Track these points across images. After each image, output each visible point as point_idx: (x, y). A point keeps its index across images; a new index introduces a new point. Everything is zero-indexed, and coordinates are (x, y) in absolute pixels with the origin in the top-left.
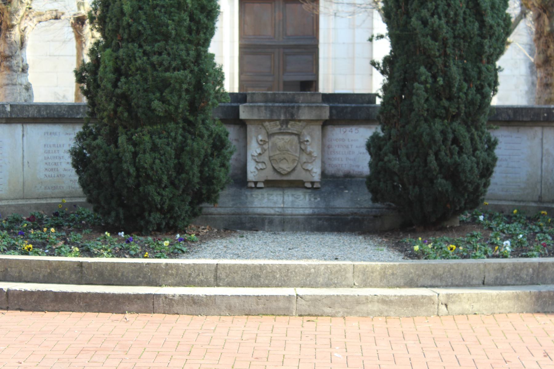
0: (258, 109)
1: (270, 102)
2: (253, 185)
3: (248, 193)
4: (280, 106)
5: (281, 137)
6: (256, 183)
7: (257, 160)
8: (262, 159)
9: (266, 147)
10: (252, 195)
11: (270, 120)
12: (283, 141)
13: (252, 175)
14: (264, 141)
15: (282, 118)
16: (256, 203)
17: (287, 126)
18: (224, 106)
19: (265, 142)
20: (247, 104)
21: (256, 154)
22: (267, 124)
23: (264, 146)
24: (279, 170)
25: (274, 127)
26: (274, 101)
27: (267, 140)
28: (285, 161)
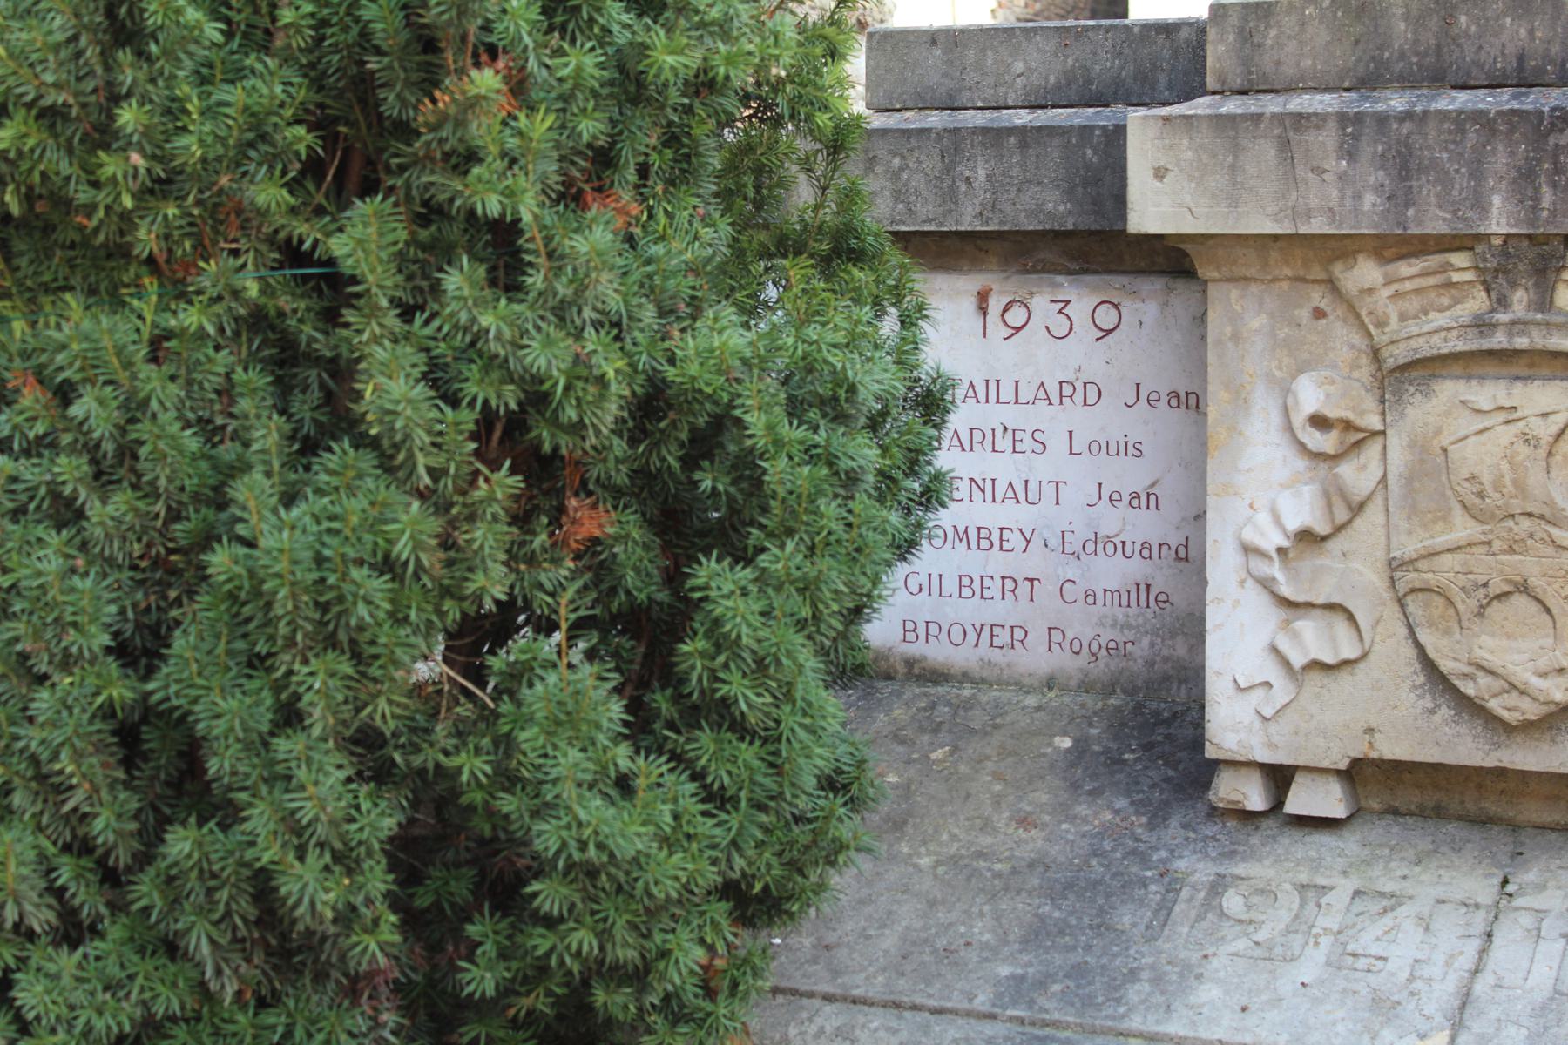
0: (1285, 145)
1: (1407, 81)
2: (1255, 798)
3: (1197, 868)
4: (1478, 116)
5: (1488, 393)
6: (1279, 777)
7: (1286, 591)
8: (1327, 577)
9: (1358, 475)
10: (1217, 887)
11: (1394, 246)
12: (1505, 434)
13: (1242, 712)
14: (1348, 426)
15: (1499, 220)
16: (1208, 993)
17: (1544, 302)
18: (1085, 130)
19: (1355, 438)
20: (1201, 106)
21: (1273, 539)
22: (1365, 273)
23: (1346, 470)
24: (1469, 689)
25: (1430, 309)
26: (1439, 77)
27: (1374, 422)
28: (1520, 601)
